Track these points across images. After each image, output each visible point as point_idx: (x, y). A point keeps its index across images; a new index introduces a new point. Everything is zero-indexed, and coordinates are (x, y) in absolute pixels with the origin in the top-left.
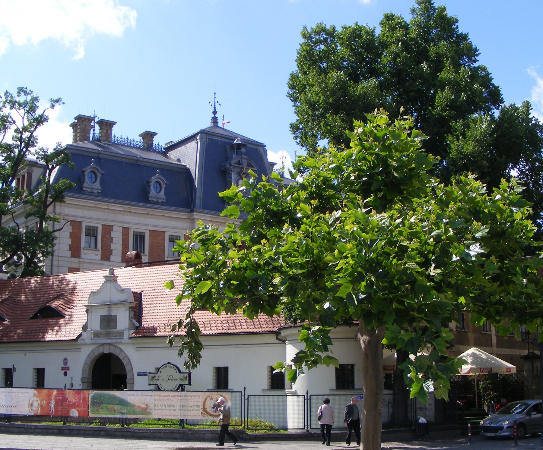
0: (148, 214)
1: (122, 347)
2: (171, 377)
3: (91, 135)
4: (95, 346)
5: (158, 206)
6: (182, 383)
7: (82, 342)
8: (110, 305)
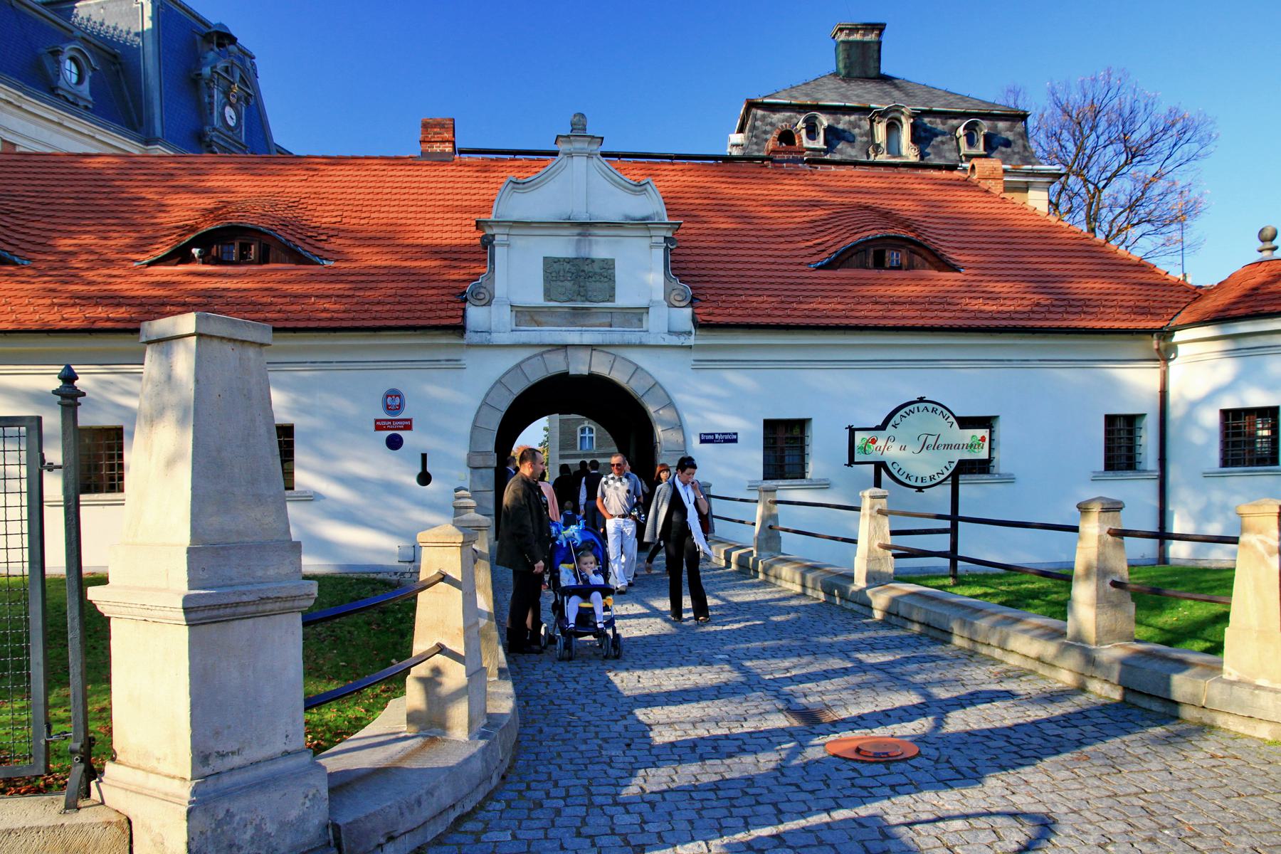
0: (60, 124)
2: (931, 441)
8: (585, 227)
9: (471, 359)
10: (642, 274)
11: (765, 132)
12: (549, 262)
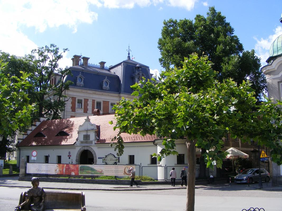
0: (102, 94)
1: (92, 147)
2: (111, 159)
3: (80, 63)
4: (81, 147)
5: (106, 91)
6: (116, 161)
7: (76, 145)
8: (87, 131)
12: (84, 135)
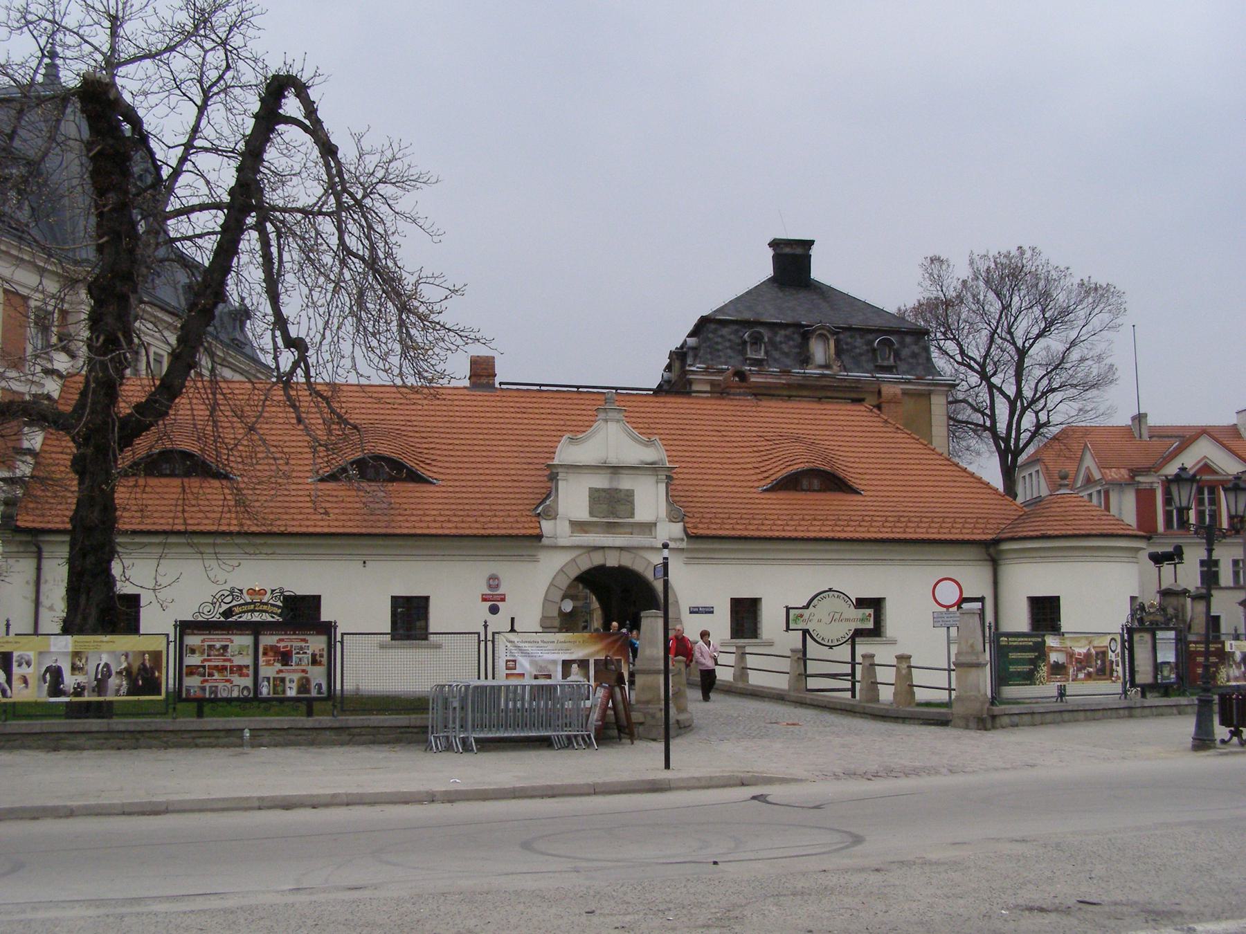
2: (837, 616)
8: (616, 470)
9: (544, 556)
10: (650, 501)
11: (717, 343)
